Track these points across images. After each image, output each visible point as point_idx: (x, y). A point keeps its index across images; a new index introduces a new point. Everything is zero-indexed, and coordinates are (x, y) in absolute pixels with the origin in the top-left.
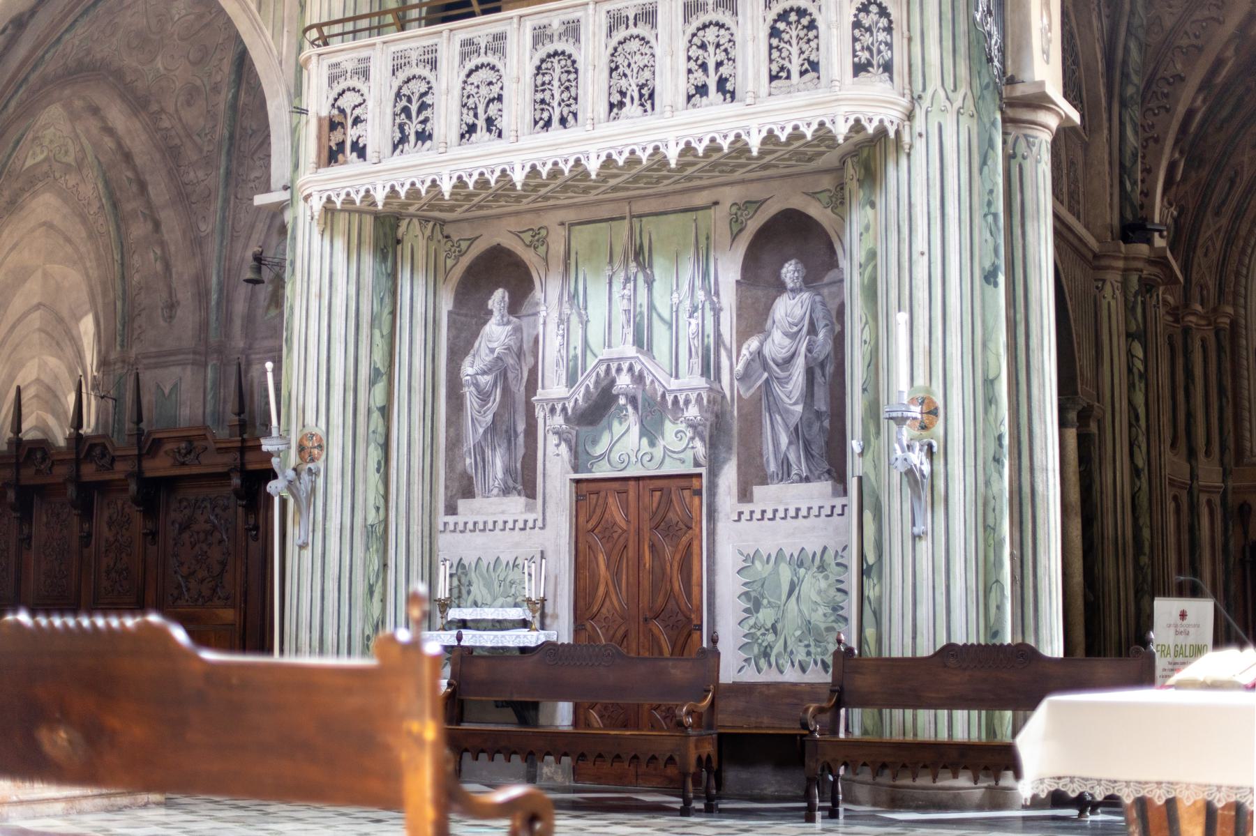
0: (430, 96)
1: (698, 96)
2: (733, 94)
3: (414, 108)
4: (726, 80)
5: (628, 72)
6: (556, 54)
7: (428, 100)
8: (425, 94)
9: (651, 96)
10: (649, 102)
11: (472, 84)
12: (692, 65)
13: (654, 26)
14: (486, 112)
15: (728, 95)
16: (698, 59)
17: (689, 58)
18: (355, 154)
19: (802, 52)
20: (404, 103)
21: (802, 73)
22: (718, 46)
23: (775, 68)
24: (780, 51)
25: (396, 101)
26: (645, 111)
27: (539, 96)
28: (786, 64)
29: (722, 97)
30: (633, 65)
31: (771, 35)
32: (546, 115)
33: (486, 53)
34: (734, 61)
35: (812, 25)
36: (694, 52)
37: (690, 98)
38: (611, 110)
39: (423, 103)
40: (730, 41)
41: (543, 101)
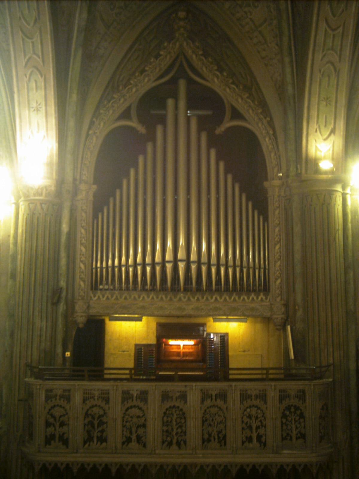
0: (105, 417)
1: (247, 442)
2: (265, 445)
3: (96, 422)
4: (261, 436)
5: (212, 423)
6: (174, 406)
7: (104, 419)
8: (102, 416)
9: (225, 437)
10: (223, 441)
11: (129, 415)
12: (244, 426)
13: (225, 402)
14: (136, 432)
15: (262, 444)
16: (247, 423)
17: (243, 422)
18: (61, 443)
19: (297, 428)
20: (90, 419)
21: (297, 438)
22: (257, 418)
23: (285, 435)
24: (287, 425)
25: (85, 417)
26: (221, 446)
27: (165, 428)
28: (290, 432)
29: (259, 445)
30: (214, 420)
31: (282, 418)
32: (169, 439)
33: (136, 400)
34: (265, 427)
35: (302, 416)
36: (246, 419)
37: (243, 443)
38: (203, 443)
39: (101, 420)
40: (263, 416)
41: (167, 431)
